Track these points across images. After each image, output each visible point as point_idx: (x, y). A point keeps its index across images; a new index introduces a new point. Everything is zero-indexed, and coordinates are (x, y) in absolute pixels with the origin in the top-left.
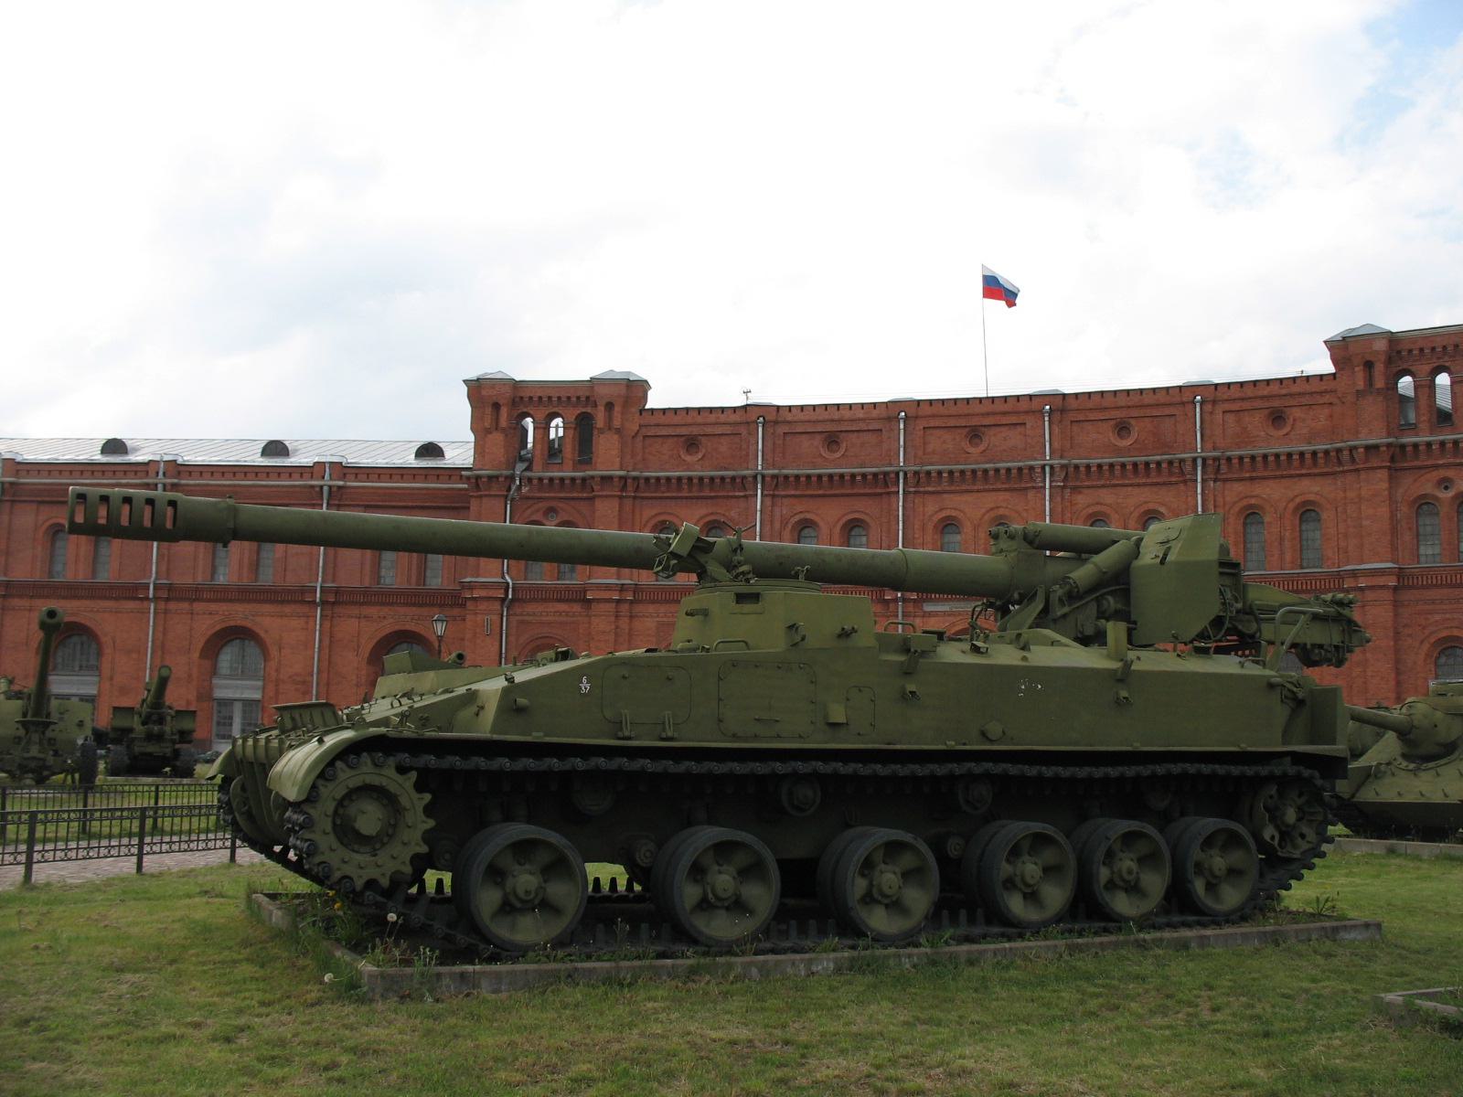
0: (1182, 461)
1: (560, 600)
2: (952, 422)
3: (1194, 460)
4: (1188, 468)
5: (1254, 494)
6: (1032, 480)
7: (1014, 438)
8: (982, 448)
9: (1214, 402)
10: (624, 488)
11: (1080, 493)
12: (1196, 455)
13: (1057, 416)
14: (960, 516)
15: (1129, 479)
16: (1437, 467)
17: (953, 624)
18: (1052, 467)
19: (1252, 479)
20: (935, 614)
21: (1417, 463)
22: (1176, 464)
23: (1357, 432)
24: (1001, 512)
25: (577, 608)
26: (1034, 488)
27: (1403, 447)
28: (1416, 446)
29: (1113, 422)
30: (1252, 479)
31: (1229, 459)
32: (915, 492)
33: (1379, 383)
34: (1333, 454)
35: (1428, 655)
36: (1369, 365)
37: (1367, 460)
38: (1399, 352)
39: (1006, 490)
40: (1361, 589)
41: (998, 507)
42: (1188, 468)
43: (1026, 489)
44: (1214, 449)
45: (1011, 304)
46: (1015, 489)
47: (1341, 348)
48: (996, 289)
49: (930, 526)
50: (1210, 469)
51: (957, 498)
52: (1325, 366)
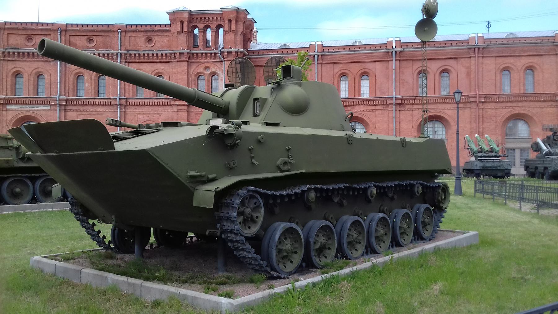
0: (112, 54)
2: (20, 32)
3: (117, 54)
4: (115, 57)
8: (33, 44)
9: (126, 32)
13: (64, 33)
16: (204, 62)
17: (19, 114)
19: (139, 62)
20: (12, 110)
21: (198, 60)
22: (110, 55)
23: (177, 47)
24: (40, 70)
27: (193, 54)
28: (197, 54)
29: (86, 37)
30: (139, 62)
31: (131, 54)
32: (4, 60)
33: (185, 29)
34: (168, 55)
36: (182, 22)
37: (180, 58)
38: (193, 18)
39: (42, 61)
40: (177, 105)
44: (125, 50)
47: (173, 14)
49: (10, 74)
50: (123, 58)
52: (166, 20)
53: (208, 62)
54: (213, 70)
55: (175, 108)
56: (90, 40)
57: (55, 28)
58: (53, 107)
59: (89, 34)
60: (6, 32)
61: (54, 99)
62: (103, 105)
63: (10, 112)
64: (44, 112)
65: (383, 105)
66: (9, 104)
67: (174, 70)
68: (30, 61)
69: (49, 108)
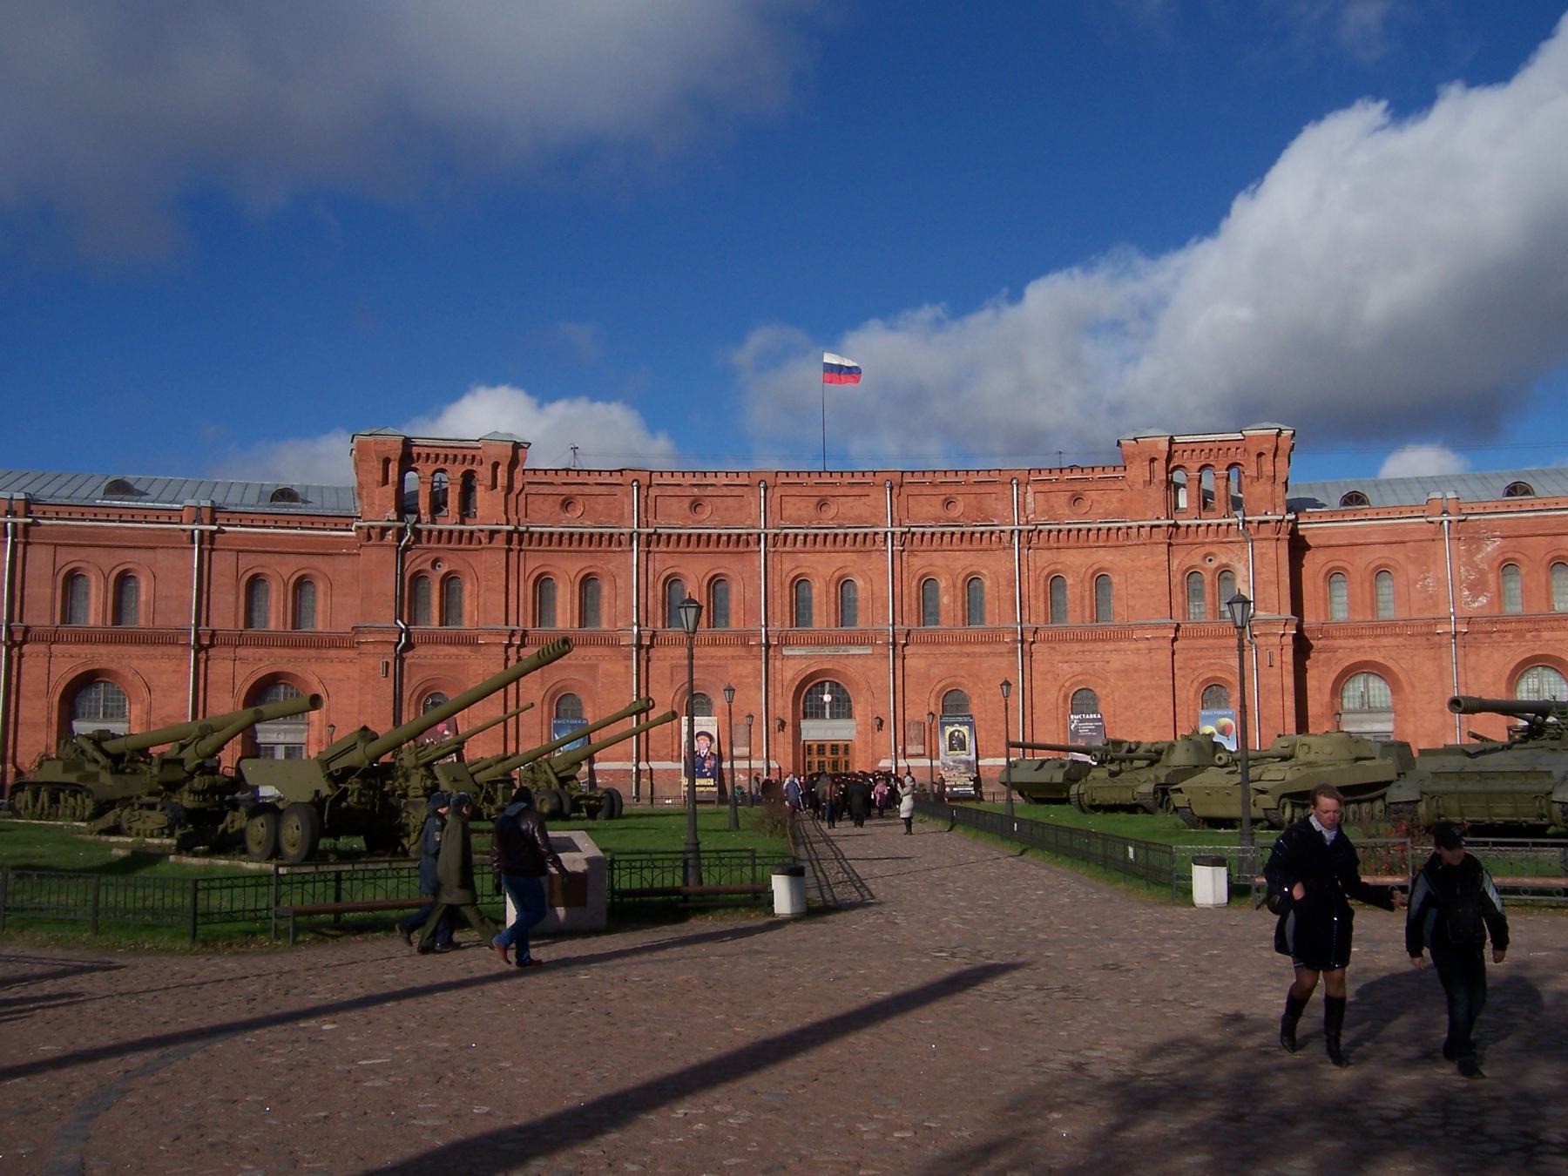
1: (450, 644)
4: (1005, 537)
7: (858, 508)
10: (509, 541)
13: (896, 491)
16: (1203, 544)
17: (809, 666)
18: (893, 534)
21: (1189, 540)
25: (466, 651)
35: (1197, 692)
44: (1027, 523)
53: (1212, 543)
54: (1225, 561)
55: (1142, 645)
56: (948, 502)
57: (879, 479)
58: (879, 650)
59: (943, 490)
61: (881, 632)
62: (982, 643)
63: (791, 662)
64: (860, 662)
67: (1138, 564)
69: (869, 651)
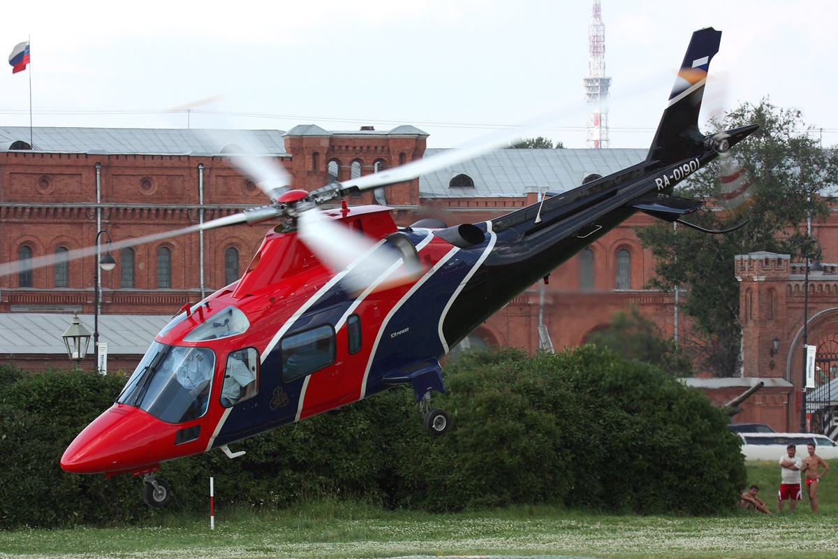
5: (235, 235)
6: (87, 217)
11: (118, 227)
12: (199, 207)
14: (36, 241)
15: (152, 220)
18: (102, 209)
22: (185, 212)
24: (64, 239)
26: (88, 223)
32: (6, 222)
36: (315, 154)
39: (68, 223)
41: (62, 236)
42: (194, 215)
43: (82, 223)
45: (15, 71)
46: (75, 223)
48: (19, 61)
49: (15, 248)
51: (32, 227)
56: (146, 182)
57: (90, 162)
60: (7, 171)
65: (657, 304)
66: (17, 303)
68: (49, 223)
